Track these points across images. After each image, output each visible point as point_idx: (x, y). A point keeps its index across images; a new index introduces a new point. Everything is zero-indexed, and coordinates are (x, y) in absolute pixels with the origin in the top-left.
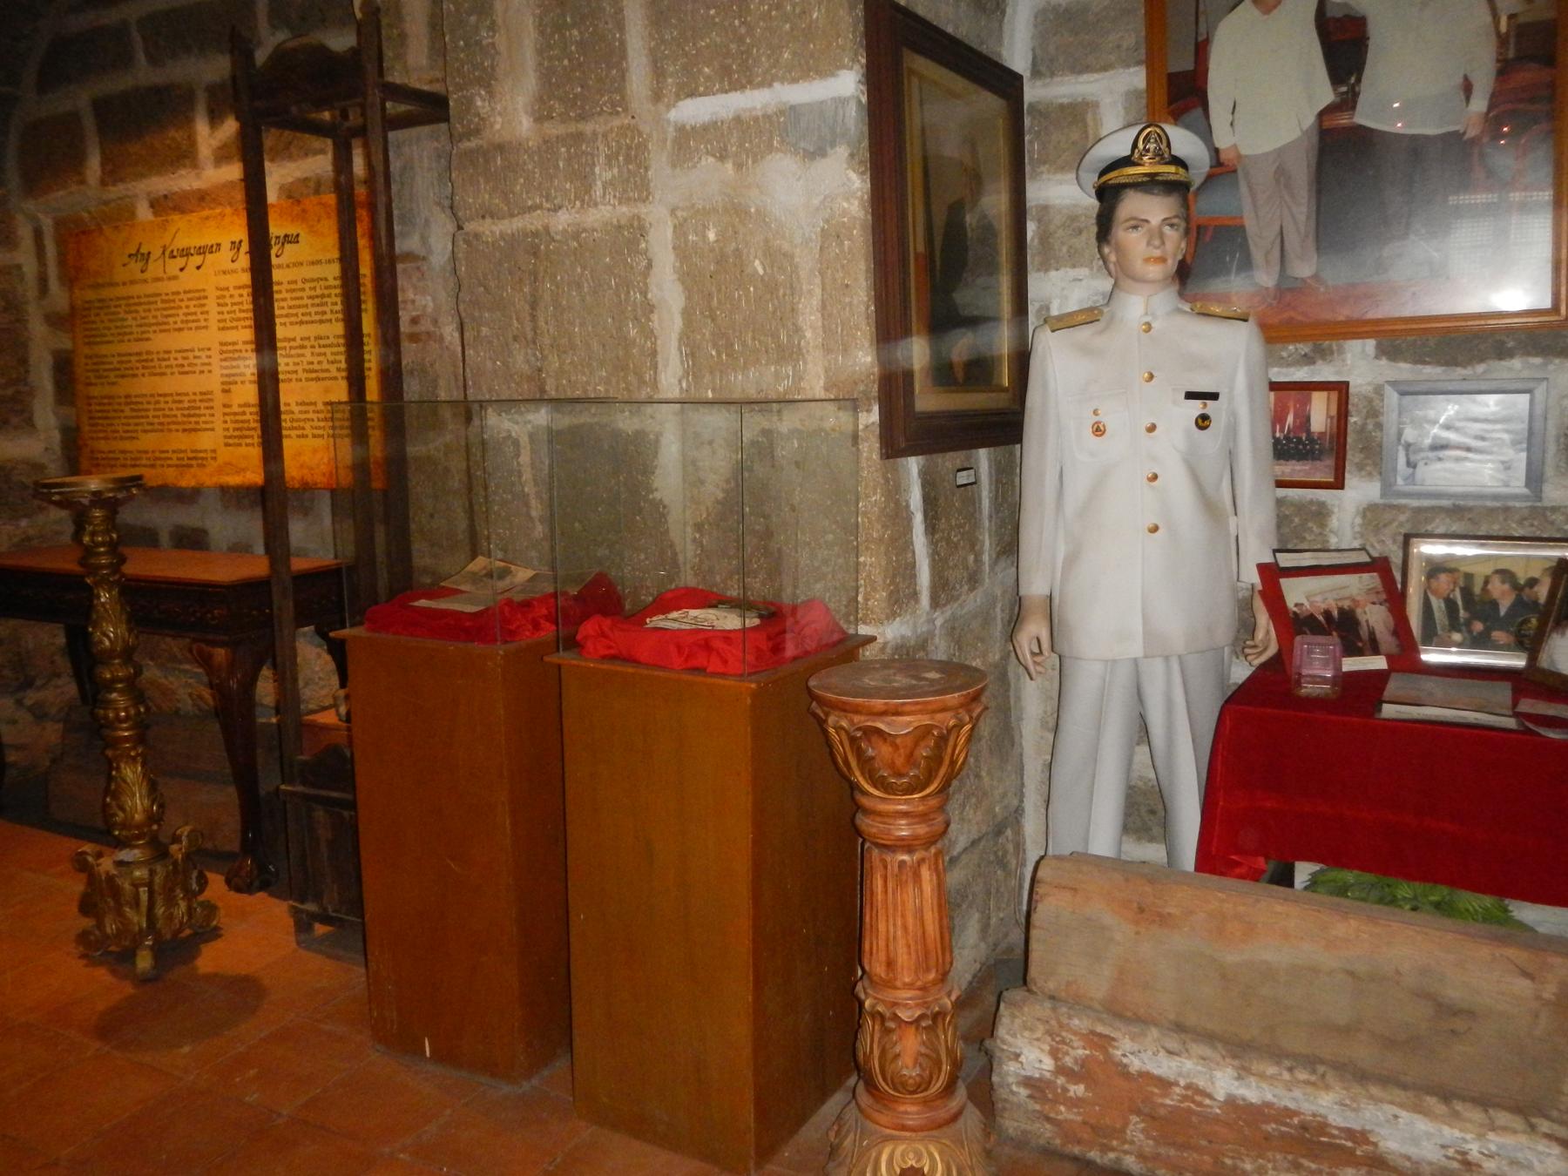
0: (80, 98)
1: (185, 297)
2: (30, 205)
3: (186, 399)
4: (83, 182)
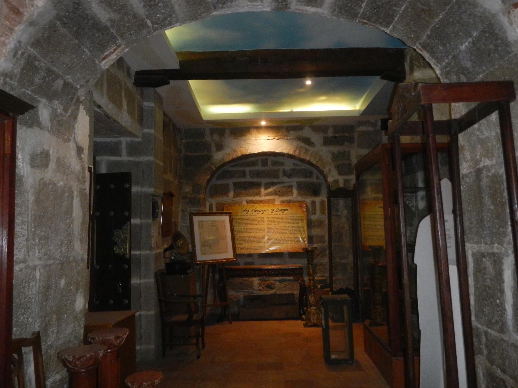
0: (230, 182)
2: (210, 200)
4: (228, 196)
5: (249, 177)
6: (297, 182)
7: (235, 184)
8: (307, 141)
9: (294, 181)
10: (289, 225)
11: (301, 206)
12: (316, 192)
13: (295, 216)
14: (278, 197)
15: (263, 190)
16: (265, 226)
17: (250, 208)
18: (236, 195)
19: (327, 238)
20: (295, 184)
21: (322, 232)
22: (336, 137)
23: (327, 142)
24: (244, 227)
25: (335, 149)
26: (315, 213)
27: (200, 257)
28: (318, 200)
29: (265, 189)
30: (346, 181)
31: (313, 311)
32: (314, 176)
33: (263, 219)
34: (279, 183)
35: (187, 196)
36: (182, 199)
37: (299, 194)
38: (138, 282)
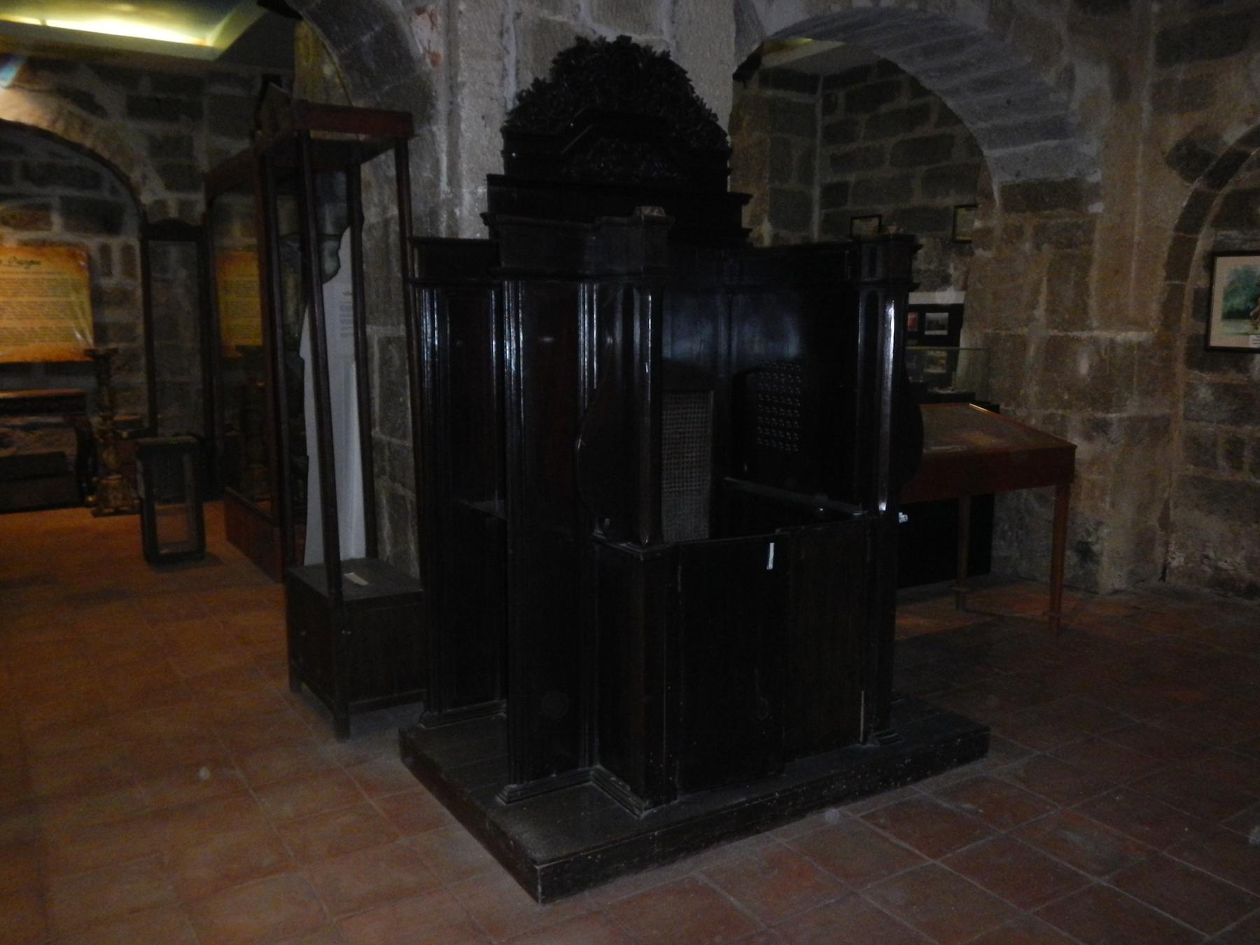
6: (61, 198)
8: (85, 101)
9: (55, 193)
11: (73, 256)
12: (108, 222)
14: (11, 230)
19: (140, 330)
20: (56, 202)
21: (129, 316)
22: (158, 100)
23: (136, 109)
25: (157, 128)
26: (109, 274)
28: (115, 243)
30: (184, 206)
31: (114, 483)
37: (67, 227)
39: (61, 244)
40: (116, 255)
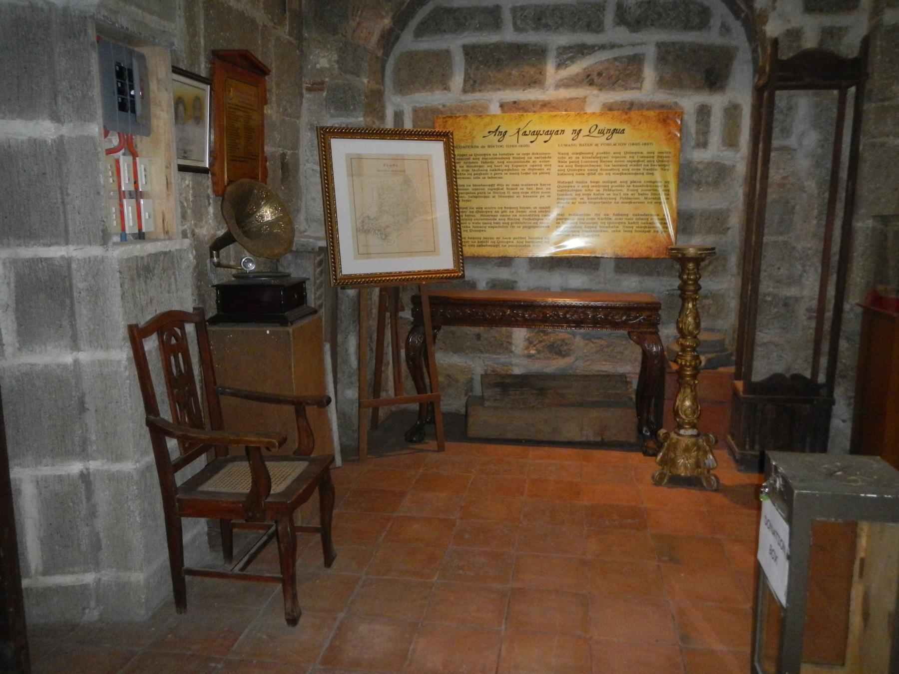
0: (454, 44)
1: (533, 157)
2: (398, 99)
3: (528, 210)
5: (511, 27)
6: (659, 45)
7: (470, 52)
9: (649, 41)
10: (625, 178)
13: (645, 150)
14: (595, 92)
15: (550, 68)
16: (553, 179)
17: (510, 124)
18: (472, 84)
19: (736, 220)
20: (651, 52)
24: (490, 182)
26: (704, 145)
27: (352, 264)
28: (717, 102)
29: (559, 66)
30: (829, 33)
31: (685, 442)
32: (715, 23)
33: (546, 157)
34: (603, 47)
35: (323, 83)
36: (309, 90)
37: (662, 83)
38: (68, 359)
39: (651, 106)
40: (717, 120)
